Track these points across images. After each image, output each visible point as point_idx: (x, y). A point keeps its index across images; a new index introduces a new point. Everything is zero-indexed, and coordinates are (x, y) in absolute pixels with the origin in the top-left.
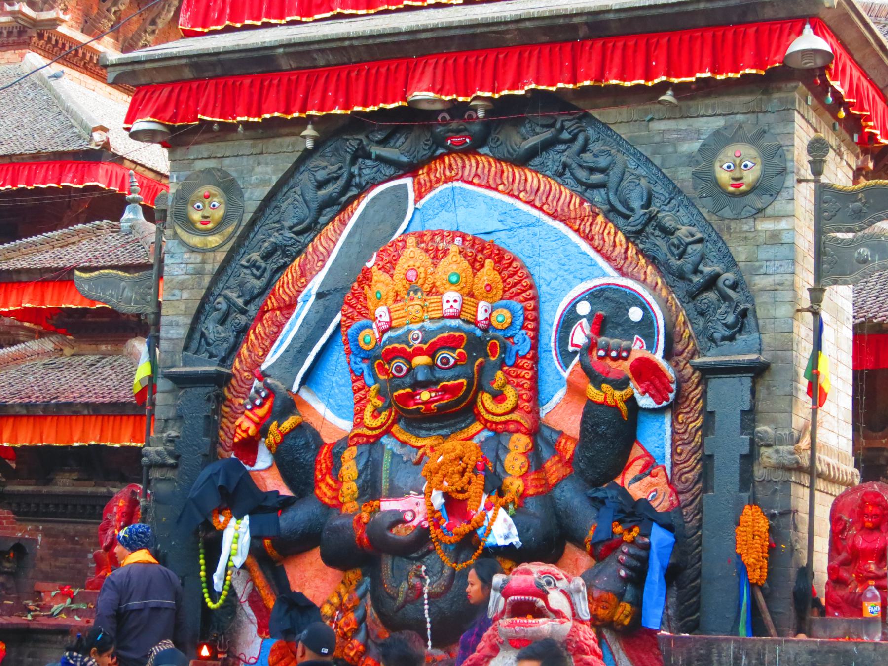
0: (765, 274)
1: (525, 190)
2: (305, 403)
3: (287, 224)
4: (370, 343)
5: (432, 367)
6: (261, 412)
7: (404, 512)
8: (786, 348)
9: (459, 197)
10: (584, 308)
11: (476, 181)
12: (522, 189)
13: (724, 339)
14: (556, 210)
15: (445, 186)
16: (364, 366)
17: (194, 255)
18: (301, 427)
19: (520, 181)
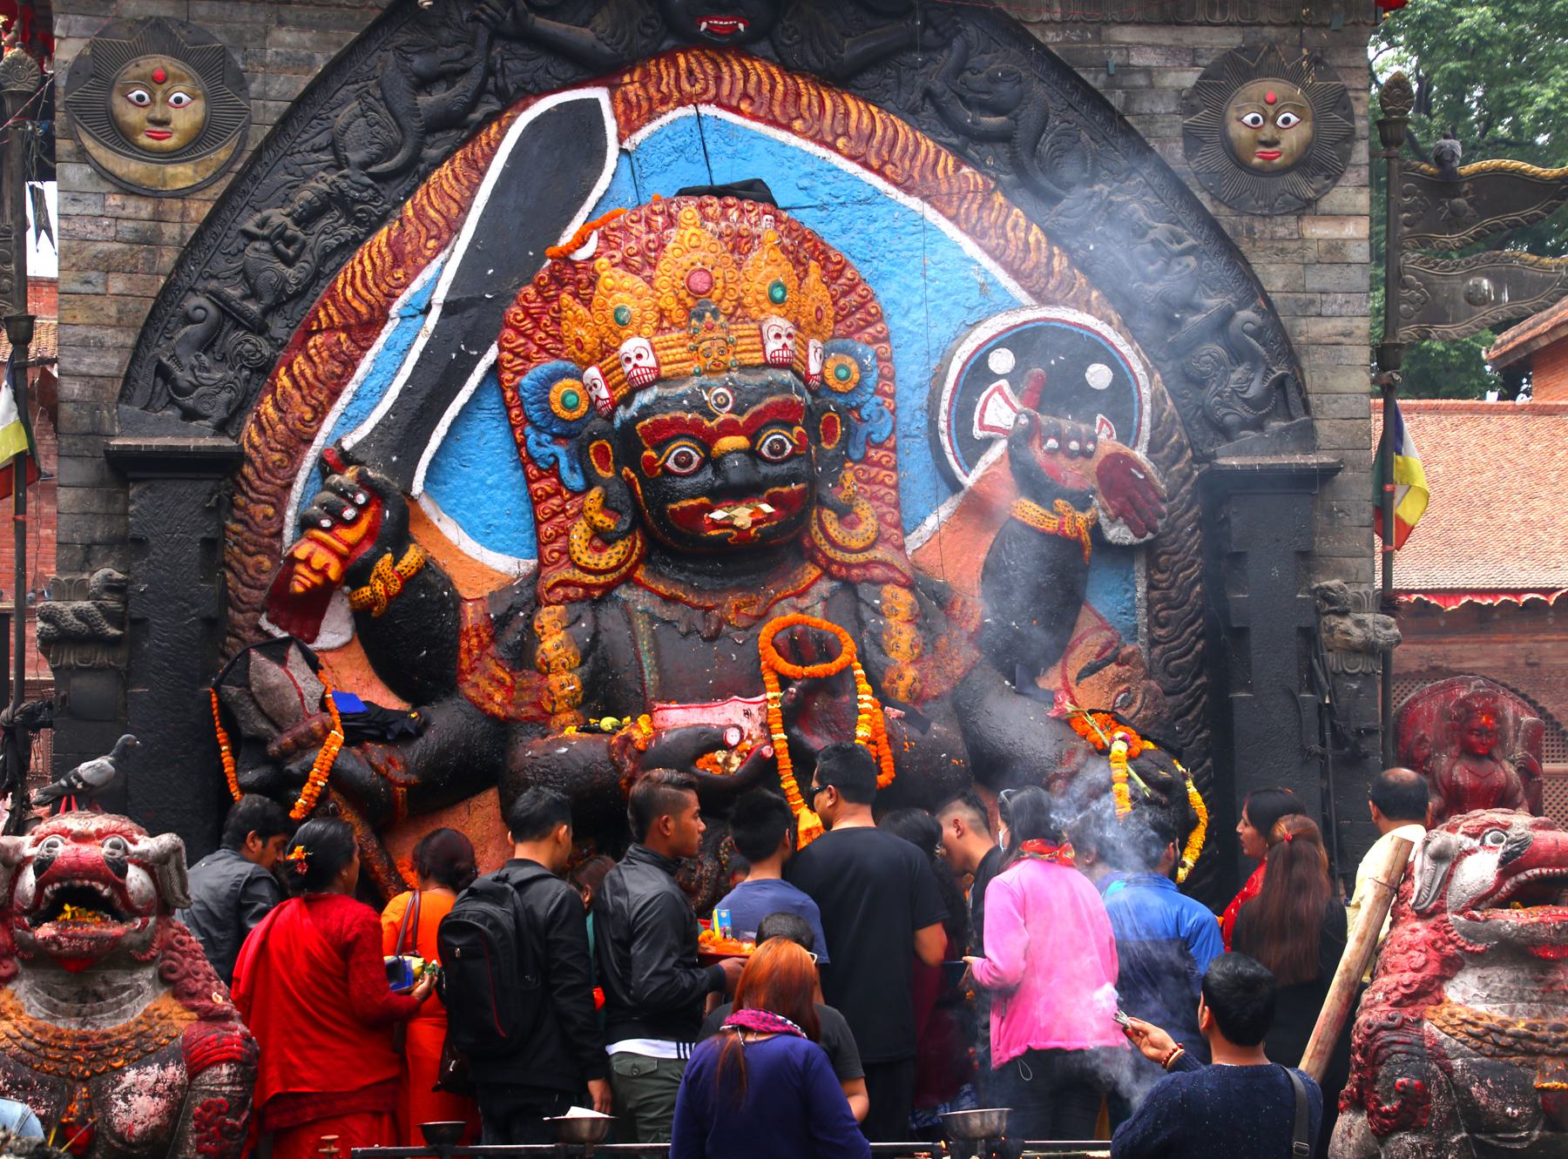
0: (1320, 315)
1: (846, 134)
2: (423, 518)
3: (354, 157)
4: (575, 407)
5: (752, 454)
6: (351, 535)
7: (724, 728)
8: (1359, 445)
9: (715, 136)
10: (1002, 361)
11: (743, 106)
12: (840, 131)
13: (1245, 425)
14: (911, 177)
15: (681, 112)
16: (559, 450)
17: (132, 203)
18: (427, 566)
19: (834, 116)
